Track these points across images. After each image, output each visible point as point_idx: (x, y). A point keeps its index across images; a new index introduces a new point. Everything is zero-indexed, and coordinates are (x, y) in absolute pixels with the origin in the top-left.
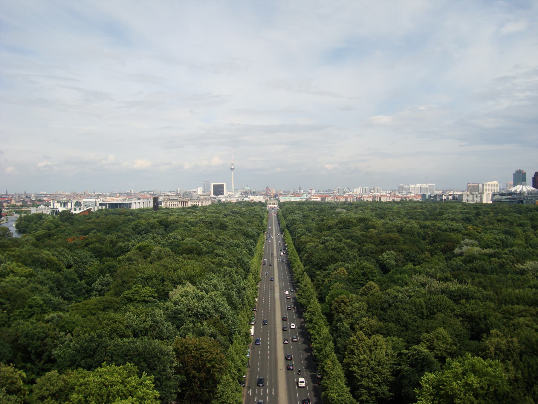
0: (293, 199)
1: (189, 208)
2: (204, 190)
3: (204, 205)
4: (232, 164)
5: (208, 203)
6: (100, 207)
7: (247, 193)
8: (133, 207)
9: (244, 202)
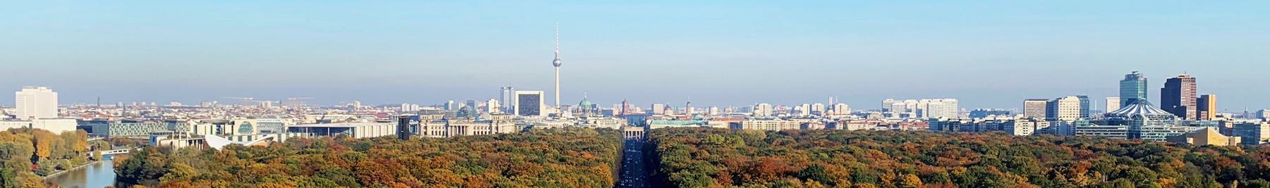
0: (677, 125)
6: (292, 135)
8: (359, 136)
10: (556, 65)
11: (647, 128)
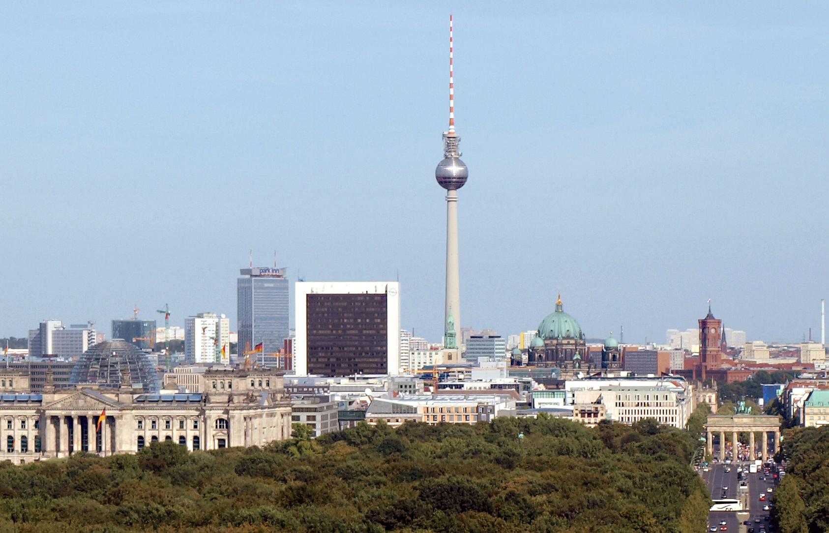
1: (120, 462)
2: (245, 334)
3: (237, 441)
4: (451, 142)
5: (265, 430)
7: (552, 358)
9: (526, 427)
10: (447, 182)
11: (790, 421)
